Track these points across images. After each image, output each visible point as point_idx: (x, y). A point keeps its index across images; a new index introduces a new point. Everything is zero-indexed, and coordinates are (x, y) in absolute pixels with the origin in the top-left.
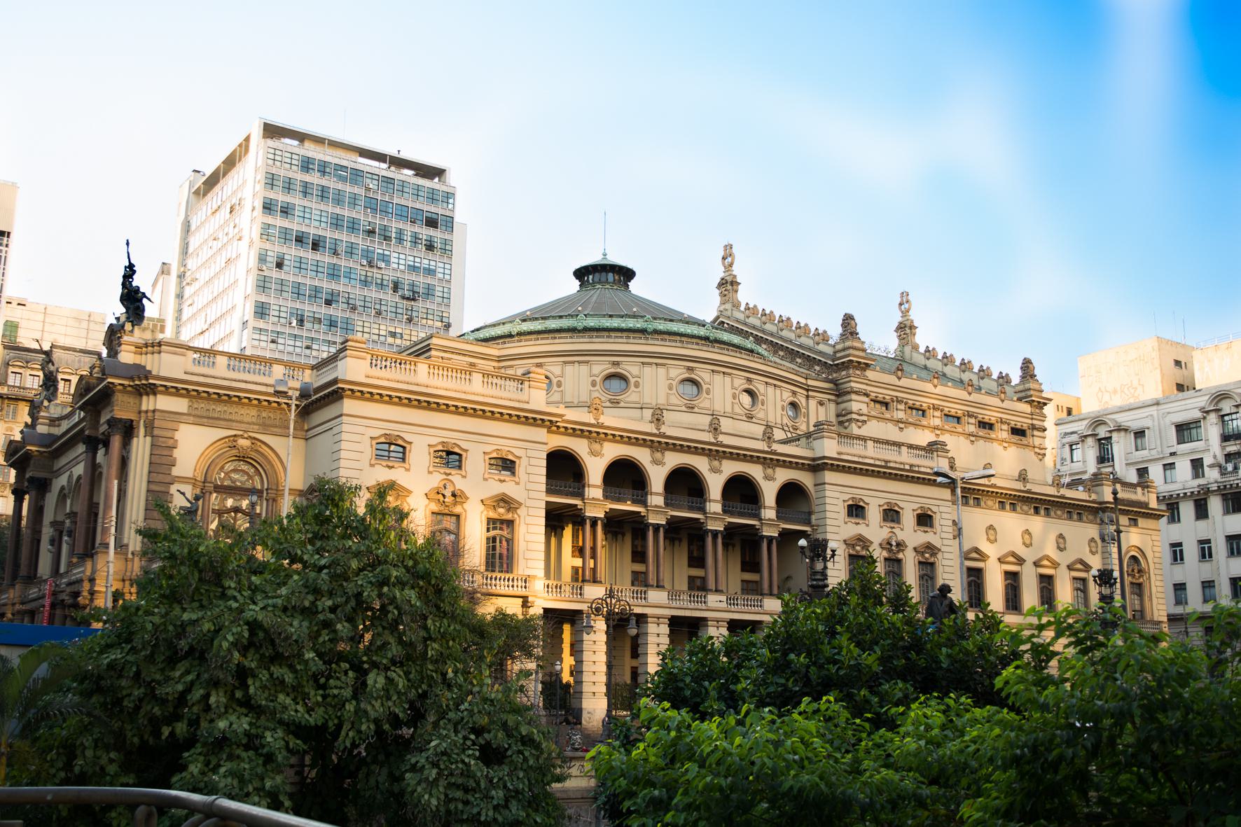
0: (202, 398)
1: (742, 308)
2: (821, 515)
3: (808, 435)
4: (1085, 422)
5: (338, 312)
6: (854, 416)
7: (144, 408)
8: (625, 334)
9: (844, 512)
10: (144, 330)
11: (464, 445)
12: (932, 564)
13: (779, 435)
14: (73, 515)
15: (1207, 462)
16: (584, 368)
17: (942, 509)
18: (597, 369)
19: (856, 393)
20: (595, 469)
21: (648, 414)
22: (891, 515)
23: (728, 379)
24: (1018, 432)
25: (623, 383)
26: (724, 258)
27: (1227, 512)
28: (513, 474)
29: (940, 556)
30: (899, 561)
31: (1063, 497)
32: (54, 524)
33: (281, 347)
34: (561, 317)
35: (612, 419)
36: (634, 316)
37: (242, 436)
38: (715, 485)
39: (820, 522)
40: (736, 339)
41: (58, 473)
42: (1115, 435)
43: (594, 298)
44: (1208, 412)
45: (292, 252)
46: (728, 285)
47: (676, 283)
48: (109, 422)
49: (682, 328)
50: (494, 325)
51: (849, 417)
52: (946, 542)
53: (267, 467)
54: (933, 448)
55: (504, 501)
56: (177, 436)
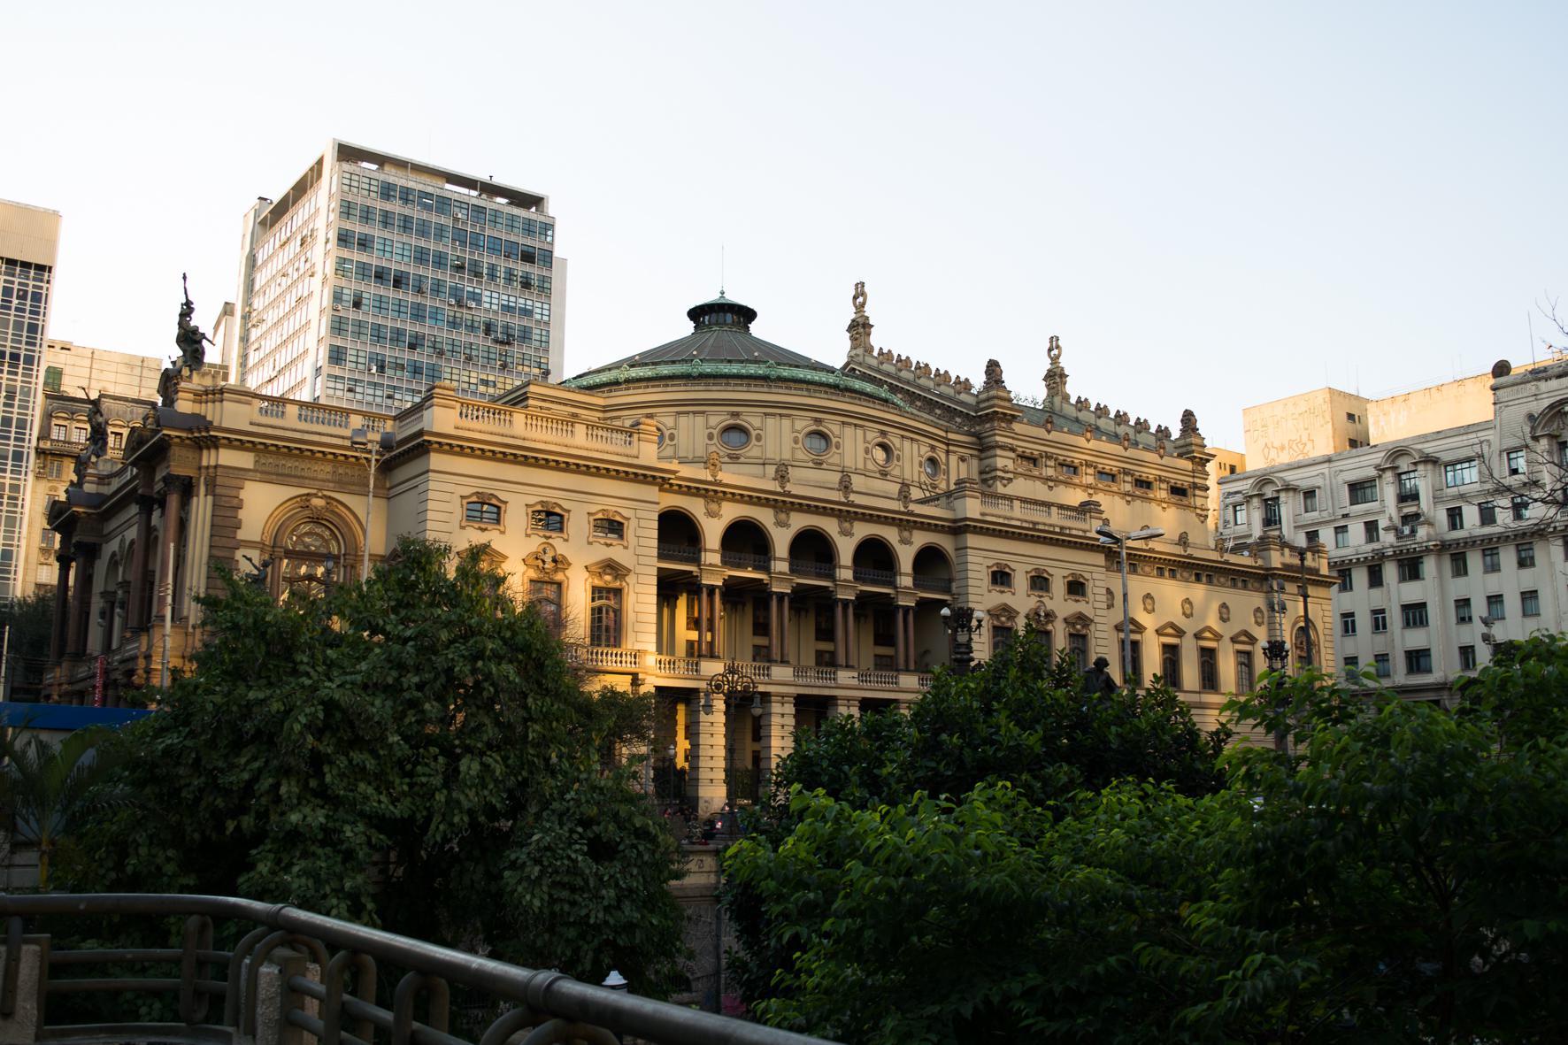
0: (270, 452)
1: (875, 353)
2: (962, 583)
3: (949, 494)
5: (423, 357)
7: (204, 463)
9: (987, 579)
10: (204, 375)
11: (565, 505)
12: (1084, 637)
13: (916, 493)
14: (125, 584)
15: (1383, 523)
16: (700, 420)
17: (1095, 576)
18: (714, 420)
19: (1002, 447)
20: (713, 531)
21: (771, 470)
23: (860, 432)
24: (1178, 491)
25: (743, 437)
26: (855, 298)
27: (1403, 579)
28: (621, 537)
29: (1092, 627)
30: (1048, 633)
31: (1226, 562)
32: (104, 594)
33: (359, 397)
34: (674, 362)
35: (730, 476)
36: (756, 361)
37: (315, 495)
38: (846, 549)
39: (961, 591)
40: (869, 388)
41: (108, 538)
42: (1283, 496)
44: (1384, 470)
45: (371, 290)
46: (860, 328)
47: (802, 326)
48: (164, 479)
50: (599, 371)
52: (1099, 612)
53: (345, 530)
54: (1087, 509)
55: (611, 567)
56: (243, 494)
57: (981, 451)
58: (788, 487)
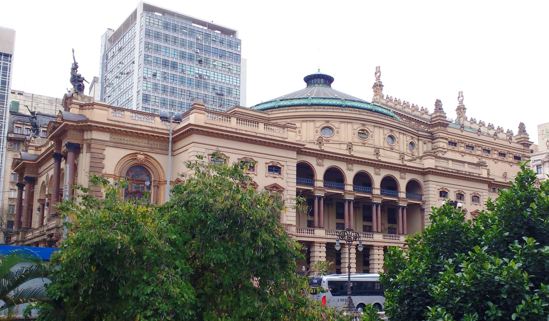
4: (545, 155)
6: (441, 149)
7: (85, 137)
8: (332, 107)
13: (406, 158)
14: (49, 195)
16: (312, 124)
18: (318, 124)
20: (320, 173)
21: (345, 147)
23: (381, 130)
24: (517, 158)
28: (280, 174)
32: (40, 200)
34: (300, 99)
35: (327, 148)
38: (377, 181)
40: (385, 111)
43: (315, 90)
46: (378, 86)
48: (66, 145)
49: (359, 105)
51: (438, 149)
56: (105, 153)
57: (433, 139)
58: (352, 153)
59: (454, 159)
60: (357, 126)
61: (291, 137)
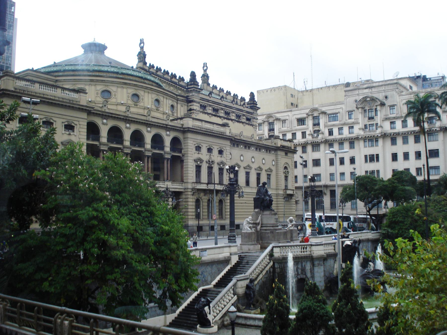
2: (186, 150)
3: (181, 119)
17: (227, 148)
22: (210, 150)
25: (109, 94)
26: (140, 44)
27: (313, 151)
42: (275, 122)
51: (192, 111)
52: (228, 161)
54: (224, 125)
57: (188, 103)
59: (203, 120)
60: (131, 91)
61: (83, 100)
